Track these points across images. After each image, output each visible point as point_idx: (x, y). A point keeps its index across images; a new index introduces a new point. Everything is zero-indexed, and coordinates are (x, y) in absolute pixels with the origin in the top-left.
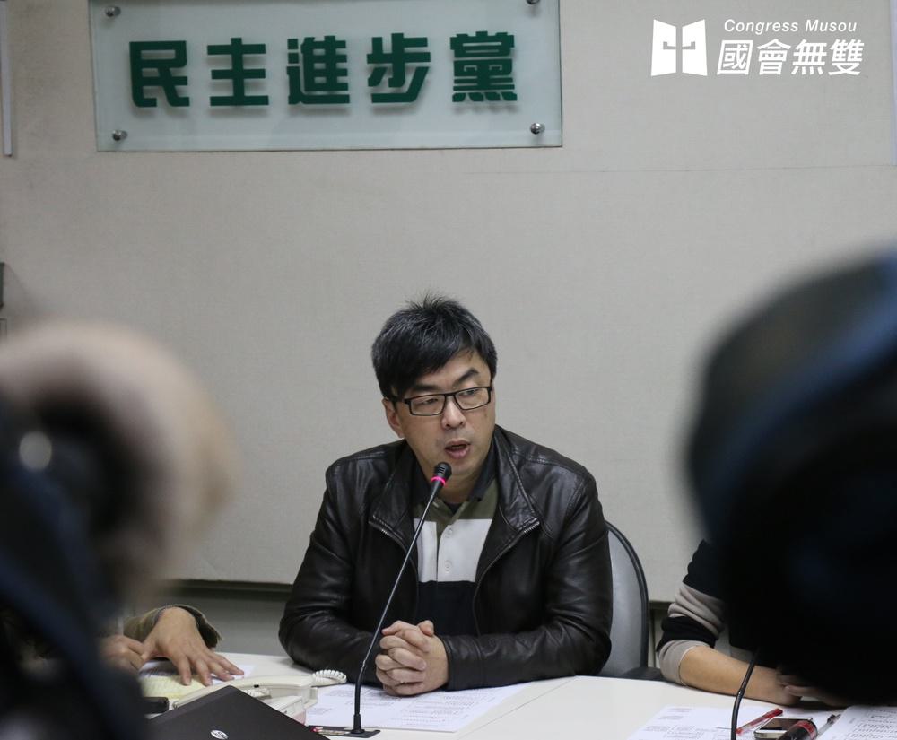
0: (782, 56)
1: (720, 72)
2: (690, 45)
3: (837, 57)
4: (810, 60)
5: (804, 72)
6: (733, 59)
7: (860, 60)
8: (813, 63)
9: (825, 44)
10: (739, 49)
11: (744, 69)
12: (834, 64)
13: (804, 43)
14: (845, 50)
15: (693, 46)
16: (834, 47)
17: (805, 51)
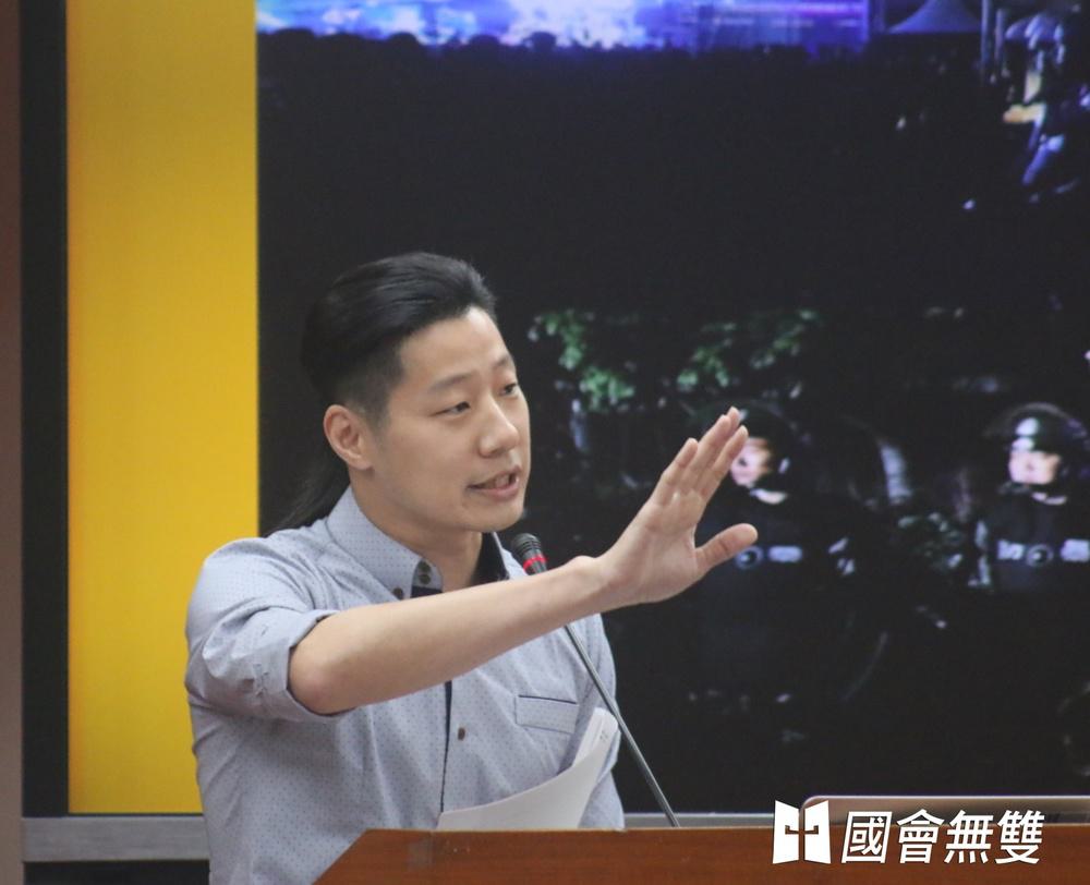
0: (931, 834)
1: (845, 859)
2: (812, 829)
3: (1008, 837)
4: (970, 841)
5: (961, 860)
6: (863, 840)
7: (1039, 841)
8: (974, 845)
9: (991, 818)
10: (871, 825)
11: (880, 854)
12: (1003, 847)
13: (961, 816)
14: (1018, 826)
15: (816, 831)
16: (1003, 822)
17: (963, 828)
